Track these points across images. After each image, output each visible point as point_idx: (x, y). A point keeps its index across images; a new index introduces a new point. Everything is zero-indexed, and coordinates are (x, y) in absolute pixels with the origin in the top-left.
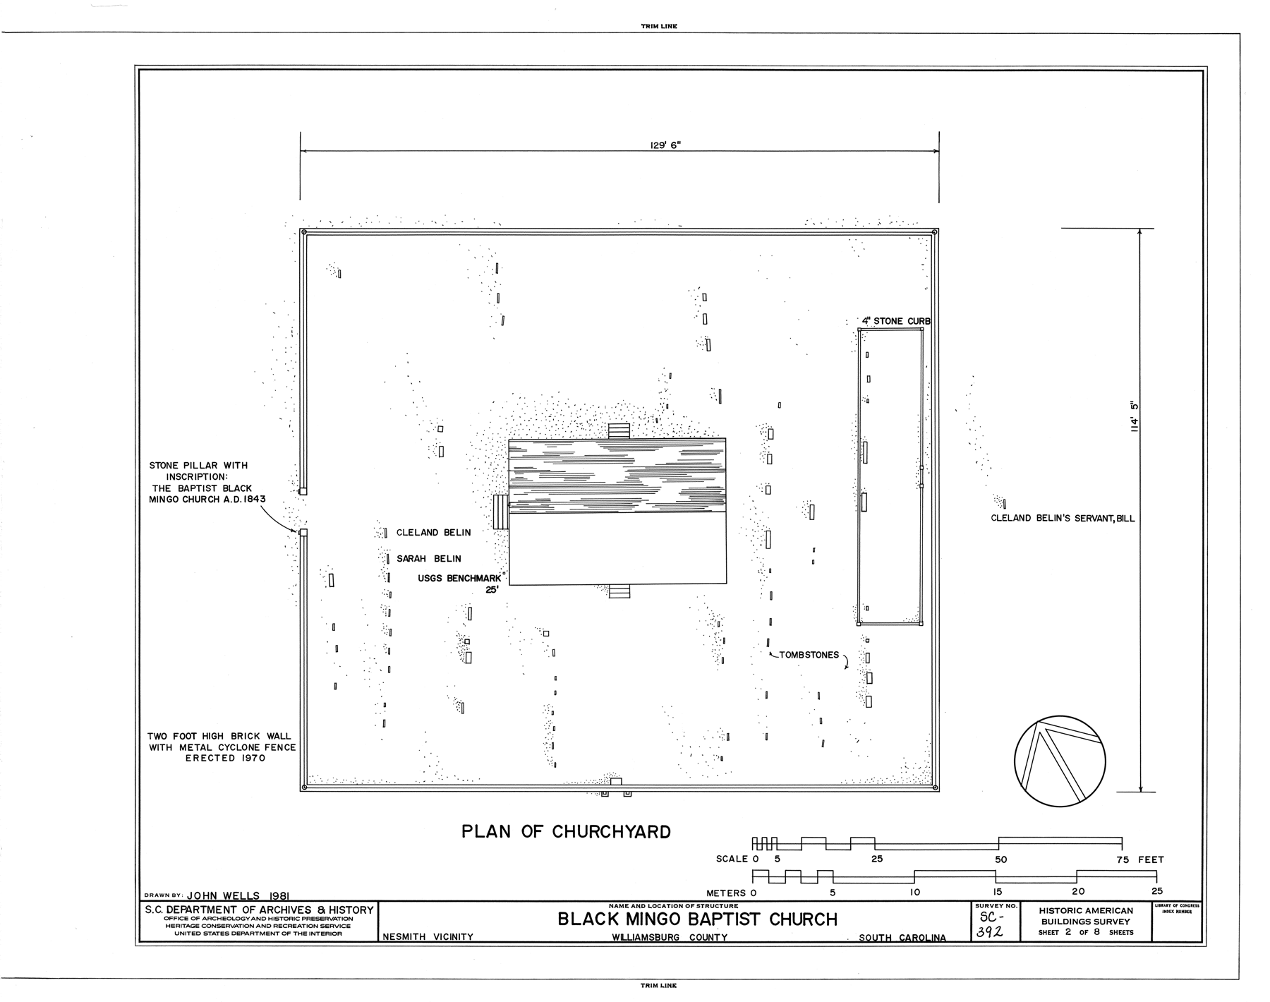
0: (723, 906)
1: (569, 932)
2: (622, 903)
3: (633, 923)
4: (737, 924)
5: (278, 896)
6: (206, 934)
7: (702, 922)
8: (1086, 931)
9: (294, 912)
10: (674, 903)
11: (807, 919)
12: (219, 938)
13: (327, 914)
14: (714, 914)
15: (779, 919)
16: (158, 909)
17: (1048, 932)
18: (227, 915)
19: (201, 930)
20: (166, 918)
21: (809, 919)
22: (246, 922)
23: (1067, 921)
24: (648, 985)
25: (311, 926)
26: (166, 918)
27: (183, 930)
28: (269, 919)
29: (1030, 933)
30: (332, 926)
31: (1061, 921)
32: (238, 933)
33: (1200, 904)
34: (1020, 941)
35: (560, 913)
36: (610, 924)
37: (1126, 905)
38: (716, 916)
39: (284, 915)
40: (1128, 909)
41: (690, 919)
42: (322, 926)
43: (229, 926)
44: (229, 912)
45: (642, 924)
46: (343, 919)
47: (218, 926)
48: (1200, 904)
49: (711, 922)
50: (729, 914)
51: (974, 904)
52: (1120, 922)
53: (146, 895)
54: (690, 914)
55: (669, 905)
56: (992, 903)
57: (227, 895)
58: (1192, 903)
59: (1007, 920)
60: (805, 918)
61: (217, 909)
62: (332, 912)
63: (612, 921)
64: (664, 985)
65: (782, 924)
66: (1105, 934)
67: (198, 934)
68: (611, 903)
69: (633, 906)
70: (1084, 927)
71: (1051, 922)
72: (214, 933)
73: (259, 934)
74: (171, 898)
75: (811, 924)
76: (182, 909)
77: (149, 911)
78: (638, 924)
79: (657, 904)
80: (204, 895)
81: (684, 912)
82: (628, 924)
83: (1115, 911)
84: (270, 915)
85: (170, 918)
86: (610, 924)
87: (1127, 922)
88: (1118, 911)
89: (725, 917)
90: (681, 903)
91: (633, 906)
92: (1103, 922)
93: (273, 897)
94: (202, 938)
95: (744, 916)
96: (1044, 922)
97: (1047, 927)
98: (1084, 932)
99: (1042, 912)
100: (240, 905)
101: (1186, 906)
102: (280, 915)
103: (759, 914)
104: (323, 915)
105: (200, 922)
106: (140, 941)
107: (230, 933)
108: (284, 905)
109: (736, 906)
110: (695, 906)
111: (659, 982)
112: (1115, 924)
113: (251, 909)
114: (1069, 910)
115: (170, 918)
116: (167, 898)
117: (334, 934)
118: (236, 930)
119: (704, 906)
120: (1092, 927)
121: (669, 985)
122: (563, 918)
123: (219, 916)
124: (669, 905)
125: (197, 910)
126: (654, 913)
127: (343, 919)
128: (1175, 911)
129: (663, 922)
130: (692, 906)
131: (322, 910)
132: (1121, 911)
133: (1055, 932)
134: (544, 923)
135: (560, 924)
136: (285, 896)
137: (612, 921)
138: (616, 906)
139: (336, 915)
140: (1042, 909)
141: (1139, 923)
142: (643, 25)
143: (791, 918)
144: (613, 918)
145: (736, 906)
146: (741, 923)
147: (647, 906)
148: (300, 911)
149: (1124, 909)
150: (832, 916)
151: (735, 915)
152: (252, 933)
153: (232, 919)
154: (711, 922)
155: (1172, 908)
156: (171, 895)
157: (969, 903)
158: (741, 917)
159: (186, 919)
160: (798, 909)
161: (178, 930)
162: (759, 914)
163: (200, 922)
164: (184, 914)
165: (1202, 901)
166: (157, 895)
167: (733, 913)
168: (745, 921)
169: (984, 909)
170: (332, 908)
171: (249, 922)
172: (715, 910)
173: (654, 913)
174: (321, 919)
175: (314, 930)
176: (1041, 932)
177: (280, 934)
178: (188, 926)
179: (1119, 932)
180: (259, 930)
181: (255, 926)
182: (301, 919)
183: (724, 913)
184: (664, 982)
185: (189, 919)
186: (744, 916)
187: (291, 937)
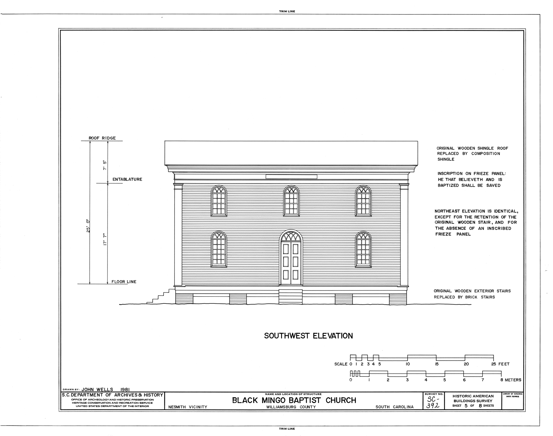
0: (315, 394)
1: (237, 406)
2: (271, 393)
3: (265, 402)
4: (310, 402)
6: (89, 406)
7: (295, 401)
8: (473, 405)
10: (293, 393)
11: (343, 400)
12: (95, 408)
14: (300, 398)
15: (330, 400)
16: (68, 395)
17: (457, 406)
18: (98, 398)
19: (88, 405)
20: (84, 400)
23: (465, 401)
24: (282, 429)
26: (84, 400)
27: (80, 404)
30: (145, 403)
31: (462, 401)
32: (104, 406)
33: (523, 393)
34: (445, 410)
36: (254, 402)
37: (491, 394)
38: (301, 399)
40: (492, 395)
41: (290, 400)
42: (140, 403)
43: (100, 403)
45: (269, 402)
46: (149, 400)
47: (95, 403)
48: (523, 393)
49: (299, 402)
50: (306, 398)
51: (424, 393)
52: (488, 401)
53: (64, 389)
54: (290, 398)
55: (291, 394)
56: (432, 393)
58: (519, 393)
59: (439, 400)
60: (343, 400)
61: (94, 395)
63: (255, 401)
64: (289, 429)
65: (331, 402)
67: (86, 406)
68: (266, 393)
69: (276, 394)
70: (472, 403)
71: (458, 401)
72: (93, 406)
73: (113, 406)
74: (74, 391)
75: (345, 402)
76: (78, 395)
78: (267, 402)
79: (286, 393)
80: (88, 389)
81: (287, 397)
83: (486, 396)
85: (74, 399)
86: (254, 402)
87: (491, 401)
88: (487, 396)
89: (305, 399)
90: (297, 393)
91: (276, 394)
92: (480, 401)
93: (122, 390)
94: (88, 408)
95: (314, 399)
96: (455, 401)
97: (456, 403)
99: (454, 397)
101: (516, 394)
105: (87, 401)
106: (61, 410)
107: (100, 406)
109: (320, 394)
110: (303, 394)
111: (287, 427)
112: (486, 402)
113: (109, 395)
114: (466, 396)
115: (74, 399)
116: (73, 391)
118: (103, 404)
119: (307, 394)
121: (292, 429)
122: (235, 400)
124: (291, 394)
125: (85, 395)
126: (274, 398)
128: (512, 396)
129: (278, 401)
130: (302, 394)
133: (460, 406)
134: (226, 401)
135: (233, 402)
137: (255, 401)
141: (496, 401)
143: (335, 400)
144: (255, 400)
145: (320, 394)
146: (312, 402)
147: (282, 394)
148: (133, 396)
149: (490, 395)
150: (354, 399)
151: (309, 398)
152: (110, 406)
153: (101, 400)
154: (299, 402)
155: (510, 395)
156: (74, 390)
157: (422, 393)
160: (339, 396)
161: (77, 404)
163: (87, 401)
164: (79, 397)
165: (523, 392)
166: (68, 389)
167: (308, 398)
168: (314, 401)
169: (430, 396)
171: (109, 401)
172: (301, 396)
173: (274, 398)
174: (140, 400)
175: (137, 405)
176: (454, 406)
177: (122, 406)
178: (82, 403)
180: (113, 404)
181: (111, 403)
182: (131, 400)
183: (305, 398)
184: (289, 427)
185: (82, 400)
186: (314, 399)
187: (127, 408)
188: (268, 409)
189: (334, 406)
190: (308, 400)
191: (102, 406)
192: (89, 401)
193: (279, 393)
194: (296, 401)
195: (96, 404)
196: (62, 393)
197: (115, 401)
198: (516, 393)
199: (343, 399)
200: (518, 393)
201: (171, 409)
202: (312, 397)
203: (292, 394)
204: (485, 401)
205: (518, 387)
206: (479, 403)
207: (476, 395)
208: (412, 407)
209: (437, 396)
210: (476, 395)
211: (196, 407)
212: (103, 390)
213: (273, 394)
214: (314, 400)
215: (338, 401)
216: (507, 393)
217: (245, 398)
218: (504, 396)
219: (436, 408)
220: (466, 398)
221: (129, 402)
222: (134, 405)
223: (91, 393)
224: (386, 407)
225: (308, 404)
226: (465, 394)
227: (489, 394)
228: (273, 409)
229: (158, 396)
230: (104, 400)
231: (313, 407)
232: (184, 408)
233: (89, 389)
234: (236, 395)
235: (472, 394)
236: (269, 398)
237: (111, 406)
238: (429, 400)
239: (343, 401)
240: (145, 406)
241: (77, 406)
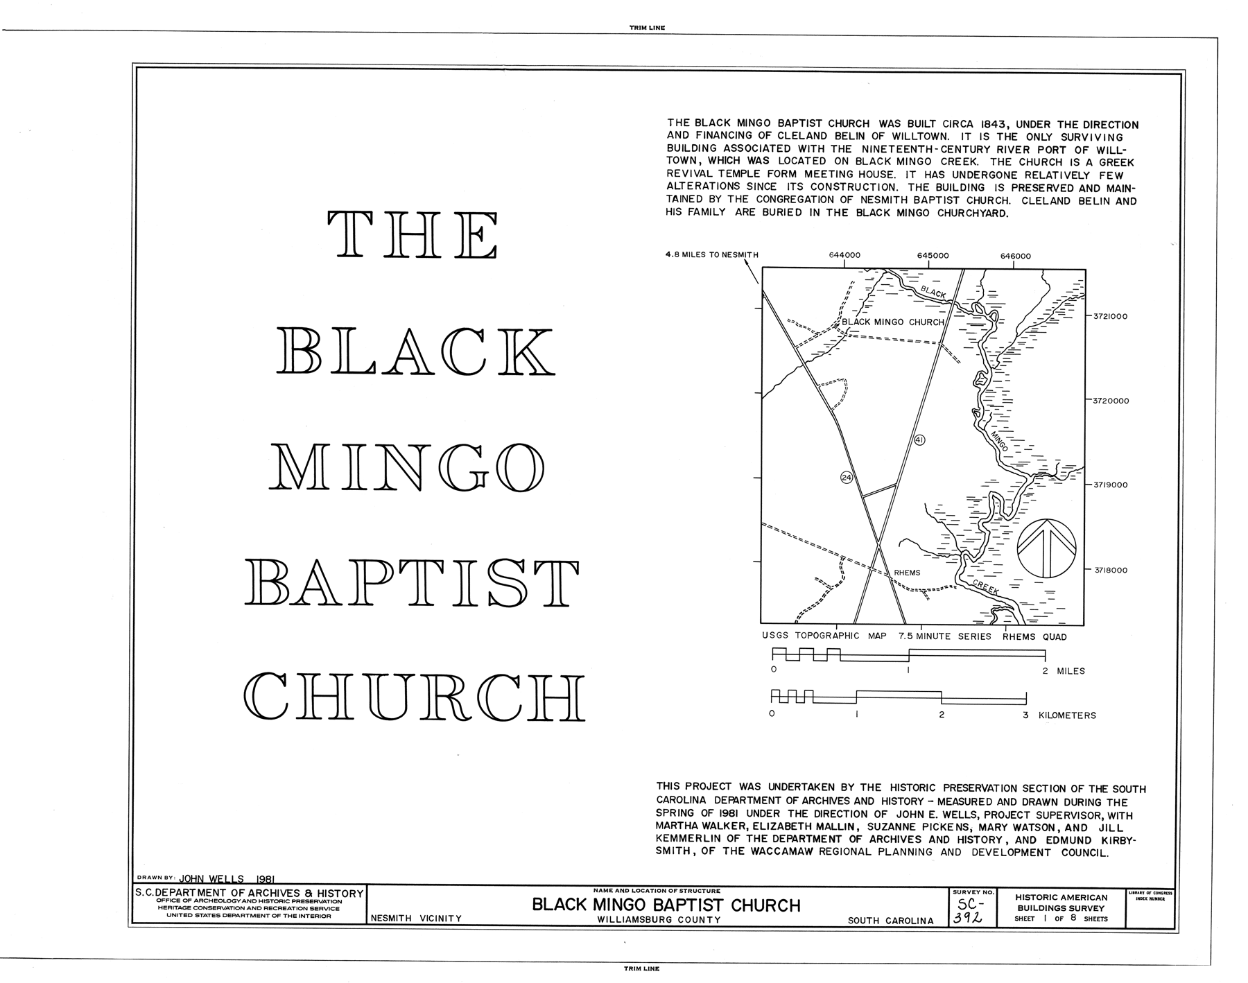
0: (705, 891)
2: (606, 888)
3: (600, 909)
4: (700, 910)
6: (197, 915)
7: (666, 907)
8: (1061, 918)
9: (283, 896)
10: (657, 888)
11: (770, 905)
13: (315, 896)
14: (678, 900)
15: (741, 905)
16: (149, 892)
17: (1024, 919)
18: (216, 897)
19: (193, 912)
21: (772, 906)
22: (237, 904)
24: (631, 968)
25: (300, 909)
27: (175, 911)
28: (260, 901)
29: (1007, 919)
30: (321, 908)
31: (1037, 908)
32: (229, 915)
33: (1173, 891)
34: (997, 927)
37: (1101, 892)
38: (680, 902)
39: (274, 897)
40: (1103, 896)
41: (655, 904)
42: (312, 909)
44: (218, 895)
46: (332, 902)
47: (210, 908)
48: (1173, 891)
49: (675, 907)
50: (692, 900)
51: (952, 890)
52: (1095, 908)
53: (139, 877)
54: (655, 900)
56: (969, 890)
58: (1165, 890)
60: (769, 904)
62: (321, 895)
64: (647, 968)
66: (1080, 922)
67: (190, 915)
68: (596, 888)
69: (617, 890)
70: (1060, 914)
71: (1027, 908)
72: (205, 915)
73: (249, 916)
74: (163, 880)
75: (774, 911)
78: (605, 909)
79: (641, 888)
82: (595, 909)
83: (1090, 898)
84: (259, 898)
87: (1101, 908)
88: (1093, 898)
90: (664, 888)
91: (617, 890)
92: (1078, 909)
95: (708, 902)
96: (1020, 908)
97: (1023, 914)
98: (1060, 918)
100: (229, 888)
101: (1159, 893)
102: (269, 897)
103: (723, 900)
104: (310, 898)
105: (192, 904)
106: (133, 923)
107: (222, 915)
108: (274, 888)
110: (678, 891)
111: (642, 966)
112: (1090, 910)
113: (241, 892)
114: (1045, 897)
115: (162, 900)
117: (324, 916)
118: (227, 912)
119: (687, 891)
120: (1067, 914)
121: (652, 969)
123: (208, 898)
124: (652, 890)
127: (332, 902)
128: (1148, 899)
130: (675, 890)
131: (309, 893)
132: (1095, 897)
133: (1031, 919)
139: (324, 898)
140: (1019, 896)
141: (1113, 909)
142: (632, 27)
146: (704, 908)
147: (631, 891)
150: (795, 902)
151: (698, 901)
152: (243, 915)
153: (223, 901)
155: (1145, 895)
156: (163, 878)
158: (705, 902)
159: (178, 901)
161: (170, 911)
162: (723, 900)
163: (192, 904)
165: (1175, 889)
166: (149, 877)
167: (696, 900)
168: (708, 907)
170: (321, 891)
171: (240, 904)
174: (311, 902)
175: (304, 912)
176: (1017, 919)
177: (270, 916)
178: (180, 908)
179: (1093, 919)
180: (249, 912)
181: (246, 908)
182: (291, 901)
183: (688, 899)
184: (647, 966)
185: (181, 901)
186: (708, 902)
188: (601, 924)
189: (749, 917)
190: (696, 904)
191: (225, 915)
192: (198, 904)
193: (625, 888)
194: (669, 905)
195: (212, 912)
197: (255, 905)
198: (1158, 891)
199: (770, 903)
200: (1164, 891)
201: (377, 922)
202: (704, 896)
206: (1075, 912)
207: (1068, 896)
208: (931, 921)
209: (979, 897)
210: (1068, 896)
211: (434, 918)
213: (611, 891)
214: (707, 905)
215: (759, 907)
216: (1137, 891)
218: (1132, 898)
219: (976, 924)
220: (1045, 903)
221: (287, 906)
222: (298, 913)
224: (872, 920)
225: (696, 913)
226: (1043, 892)
227: (1096, 892)
228: (616, 924)
230: (229, 901)
232: (408, 920)
233: (194, 877)
235: (1060, 893)
236: (609, 899)
237: (246, 916)
238: (963, 906)
239: (770, 908)
240: (321, 916)
241: (169, 915)
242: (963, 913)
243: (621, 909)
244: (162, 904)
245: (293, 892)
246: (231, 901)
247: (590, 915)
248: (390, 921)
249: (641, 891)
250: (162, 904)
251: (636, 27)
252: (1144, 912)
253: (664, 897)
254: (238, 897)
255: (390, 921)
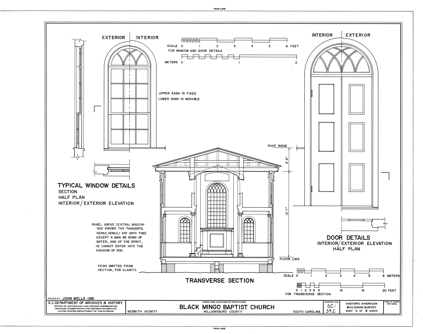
0: (241, 302)
2: (207, 301)
3: (205, 308)
5: (91, 298)
6: (68, 311)
7: (228, 308)
8: (362, 311)
10: (224, 301)
13: (107, 304)
14: (231, 305)
15: (254, 307)
17: (349, 311)
18: (75, 305)
24: (216, 328)
27: (61, 310)
28: (89, 306)
30: (110, 309)
31: (353, 307)
32: (79, 311)
33: (400, 301)
35: (180, 305)
37: (375, 302)
40: (376, 303)
41: (224, 307)
42: (107, 309)
46: (114, 306)
47: (72, 309)
48: (400, 301)
50: (236, 305)
51: (324, 301)
52: (373, 307)
53: (48, 298)
54: (224, 305)
55: (223, 302)
56: (330, 301)
57: (75, 298)
58: (397, 301)
61: (72, 303)
64: (221, 328)
66: (368, 312)
67: (66, 311)
69: (211, 302)
70: (361, 309)
71: (350, 307)
72: (71, 311)
73: (86, 311)
74: (57, 299)
76: (60, 303)
77: (49, 303)
79: (219, 301)
80: (68, 298)
83: (371, 304)
85: (56, 306)
87: (375, 307)
88: (372, 304)
90: (227, 301)
91: (211, 302)
92: (367, 308)
94: (67, 313)
96: (348, 307)
97: (349, 309)
100: (79, 301)
101: (395, 302)
103: (247, 305)
105: (66, 307)
106: (46, 314)
107: (76, 311)
108: (93, 301)
109: (245, 302)
110: (232, 302)
111: (219, 327)
112: (371, 308)
113: (82, 303)
114: (356, 303)
115: (56, 306)
116: (55, 299)
118: (78, 310)
119: (234, 302)
121: (223, 329)
124: (223, 302)
125: (65, 303)
129: (215, 308)
130: (230, 302)
132: (373, 304)
133: (351, 311)
136: (92, 298)
138: (205, 302)
141: (379, 308)
142: (214, 8)
152: (84, 311)
153: (77, 306)
155: (390, 303)
156: (57, 298)
157: (323, 301)
161: (59, 310)
162: (247, 305)
163: (66, 307)
165: (400, 301)
166: (52, 298)
171: (83, 307)
174: (107, 306)
175: (104, 310)
176: (347, 311)
178: (62, 309)
179: (373, 311)
180: (86, 310)
181: (85, 309)
182: (100, 306)
183: (235, 305)
184: (221, 328)
185: (63, 306)
187: (97, 312)
188: (205, 313)
190: (238, 307)
194: (228, 307)
195: (73, 310)
196: (47, 300)
197: (88, 308)
198: (394, 301)
200: (396, 301)
203: (223, 302)
204: (370, 308)
205: (395, 296)
206: (366, 309)
209: (334, 304)
212: (78, 299)
213: (208, 302)
217: (189, 305)
218: (386, 304)
219: (333, 313)
220: (356, 305)
222: (103, 310)
223: (70, 301)
227: (373, 302)
229: (119, 303)
231: (240, 312)
233: (68, 298)
234: (182, 303)
235: (361, 302)
237: (85, 311)
238: (329, 307)
240: (110, 311)
242: (329, 309)
243: (212, 308)
244: (56, 307)
245: (100, 302)
246: (80, 306)
247: (201, 310)
248: (133, 313)
249: (219, 302)
250: (56, 307)
251: (216, 9)
252: (390, 309)
253: (227, 304)
254: (81, 305)
255: (133, 313)
